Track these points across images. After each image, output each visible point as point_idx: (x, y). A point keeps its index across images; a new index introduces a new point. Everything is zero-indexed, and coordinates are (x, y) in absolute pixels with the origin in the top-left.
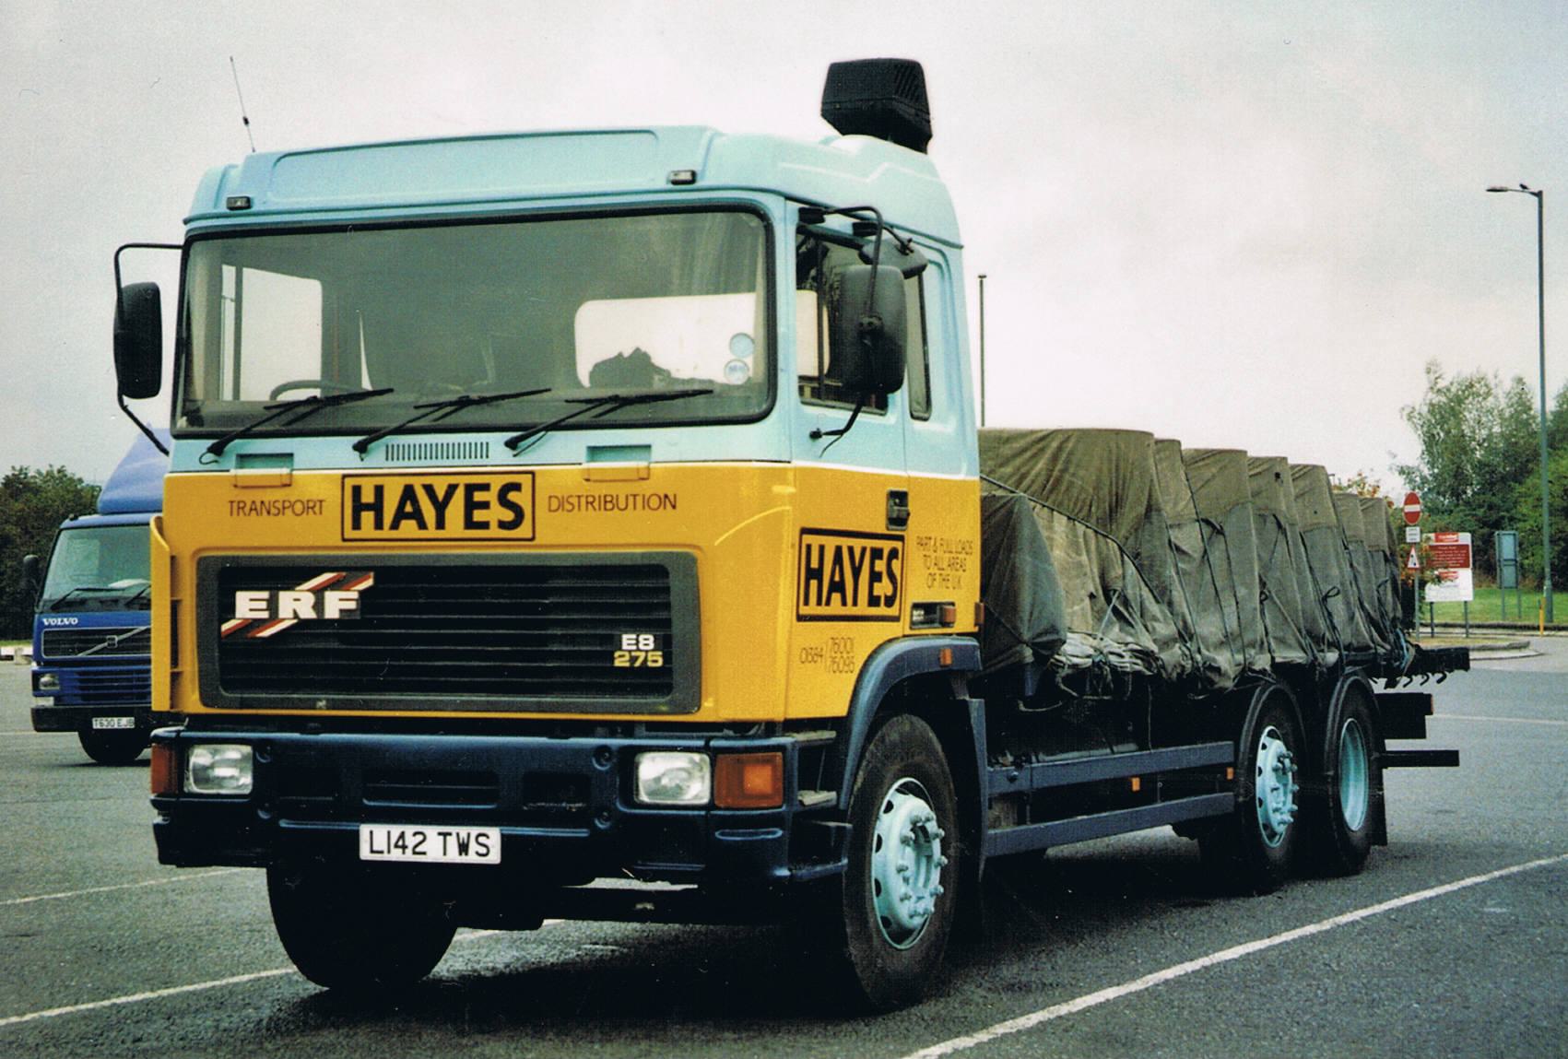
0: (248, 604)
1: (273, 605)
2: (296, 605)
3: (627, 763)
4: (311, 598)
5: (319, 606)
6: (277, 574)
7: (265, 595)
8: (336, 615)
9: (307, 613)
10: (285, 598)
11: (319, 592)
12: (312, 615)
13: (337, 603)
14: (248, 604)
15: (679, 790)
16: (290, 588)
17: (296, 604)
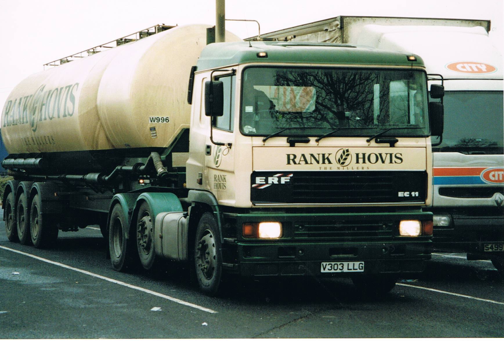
1: (266, 181)
2: (273, 180)
4: (277, 179)
5: (279, 181)
6: (267, 174)
7: (264, 178)
8: (284, 183)
9: (276, 181)
10: (270, 180)
11: (279, 178)
12: (277, 183)
13: (283, 180)
14: (259, 180)
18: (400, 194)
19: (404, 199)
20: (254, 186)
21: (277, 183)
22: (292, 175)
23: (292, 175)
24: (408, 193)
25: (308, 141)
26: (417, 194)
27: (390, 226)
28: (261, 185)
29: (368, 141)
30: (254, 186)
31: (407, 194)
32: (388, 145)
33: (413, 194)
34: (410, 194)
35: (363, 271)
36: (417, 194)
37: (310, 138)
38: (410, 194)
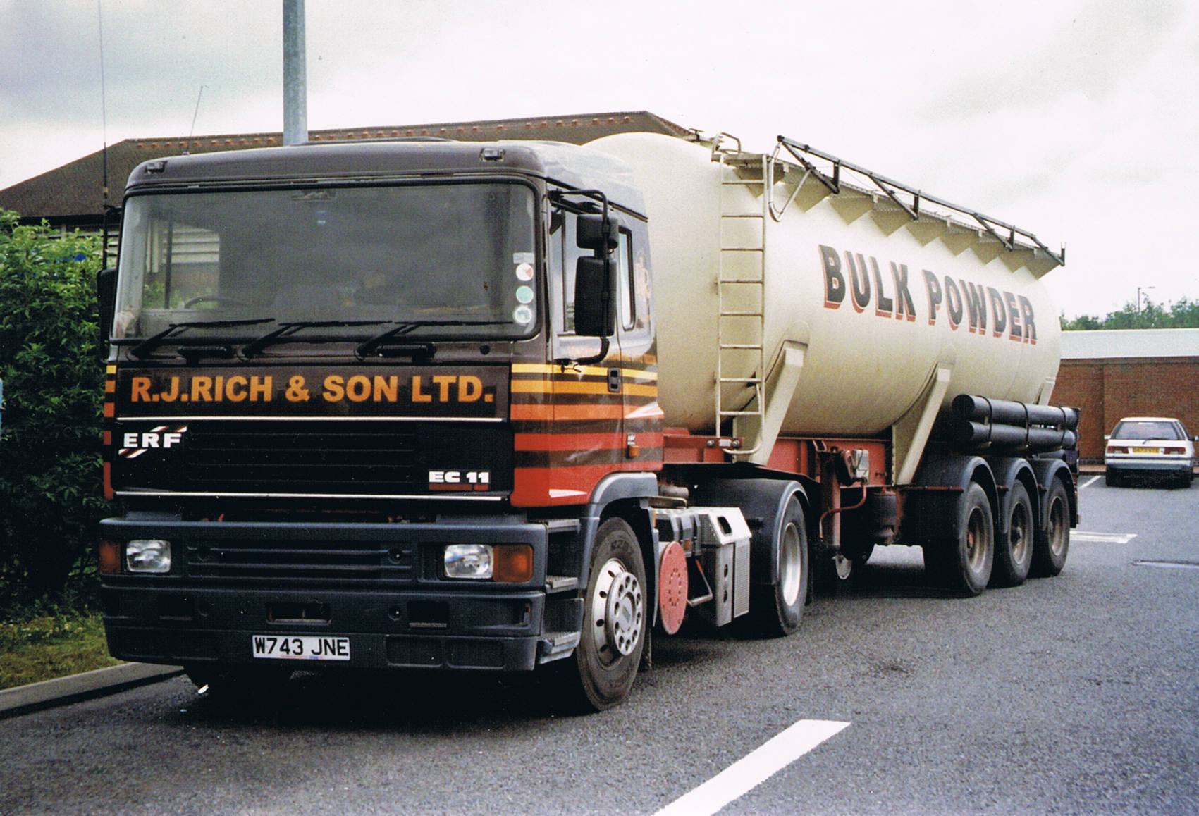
0: (129, 439)
1: (139, 440)
3: (438, 544)
4: (156, 437)
5: (161, 442)
10: (145, 436)
11: (161, 434)
12: (156, 446)
13: (169, 440)
15: (472, 569)
16: (148, 432)
17: (151, 440)
18: (435, 477)
19: (445, 488)
20: (121, 451)
21: (156, 446)
22: (184, 429)
23: (184, 429)
24: (458, 474)
25: (230, 354)
26: (485, 477)
27: (405, 555)
28: (132, 450)
29: (363, 352)
30: (121, 451)
31: (452, 477)
32: (409, 360)
33: (472, 477)
34: (464, 479)
35: (347, 658)
36: (485, 477)
37: (234, 347)
38: (464, 479)
